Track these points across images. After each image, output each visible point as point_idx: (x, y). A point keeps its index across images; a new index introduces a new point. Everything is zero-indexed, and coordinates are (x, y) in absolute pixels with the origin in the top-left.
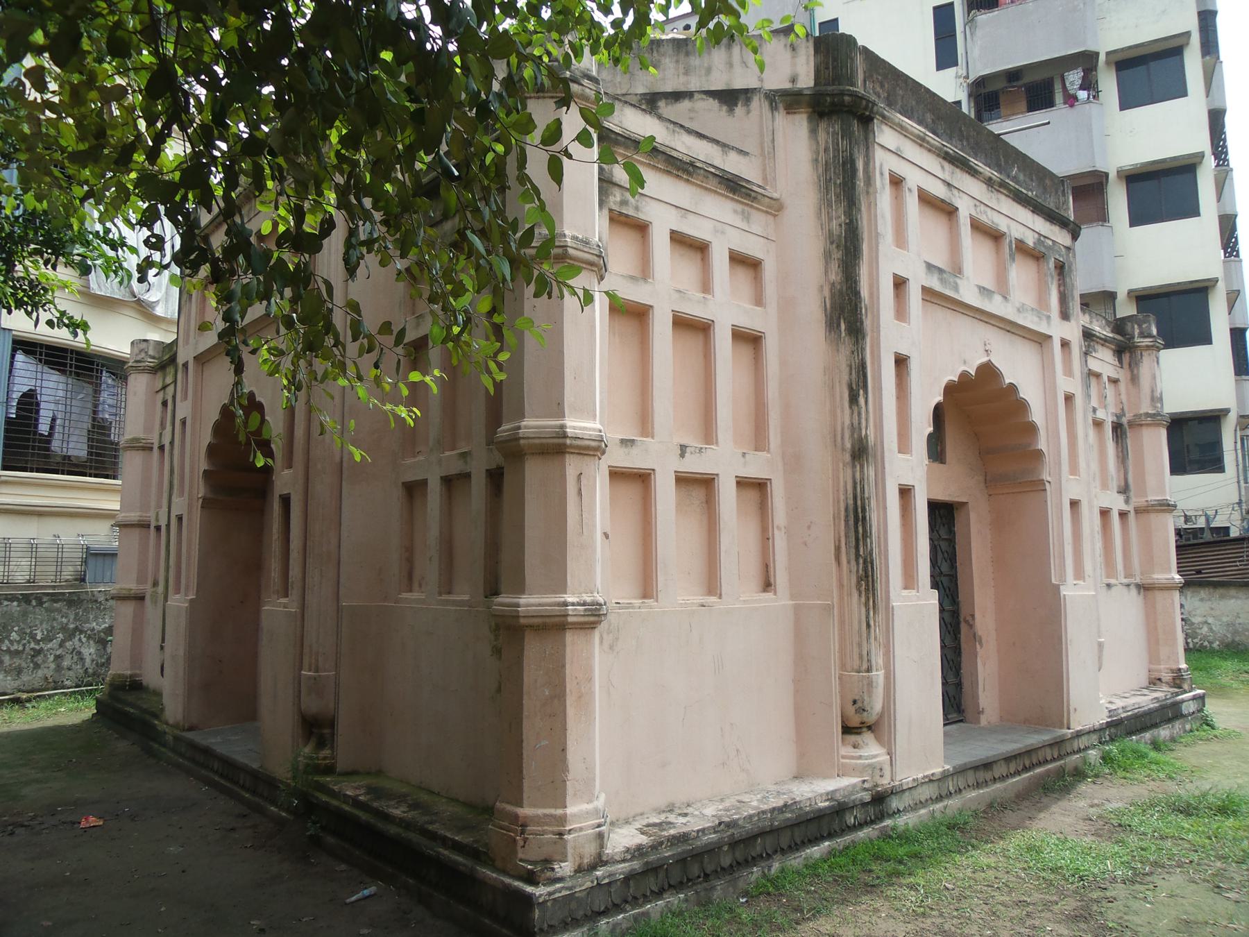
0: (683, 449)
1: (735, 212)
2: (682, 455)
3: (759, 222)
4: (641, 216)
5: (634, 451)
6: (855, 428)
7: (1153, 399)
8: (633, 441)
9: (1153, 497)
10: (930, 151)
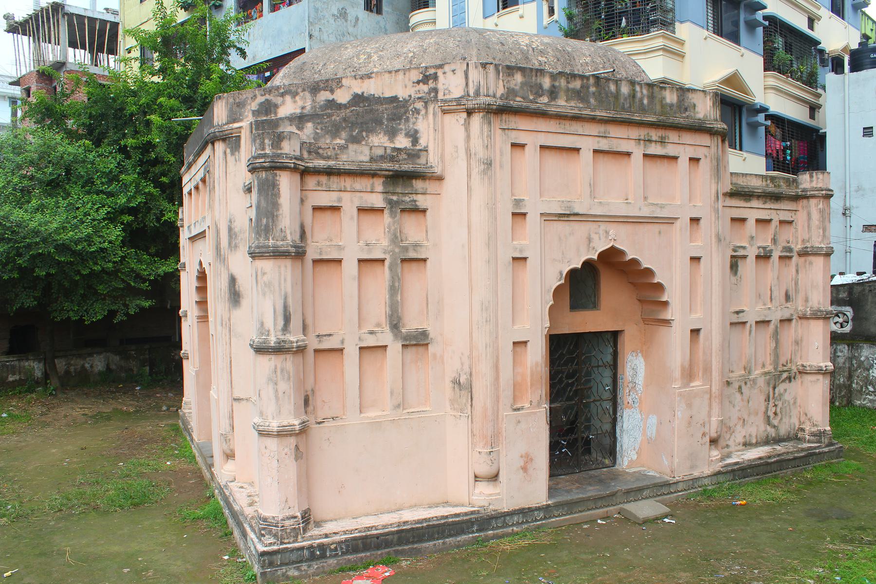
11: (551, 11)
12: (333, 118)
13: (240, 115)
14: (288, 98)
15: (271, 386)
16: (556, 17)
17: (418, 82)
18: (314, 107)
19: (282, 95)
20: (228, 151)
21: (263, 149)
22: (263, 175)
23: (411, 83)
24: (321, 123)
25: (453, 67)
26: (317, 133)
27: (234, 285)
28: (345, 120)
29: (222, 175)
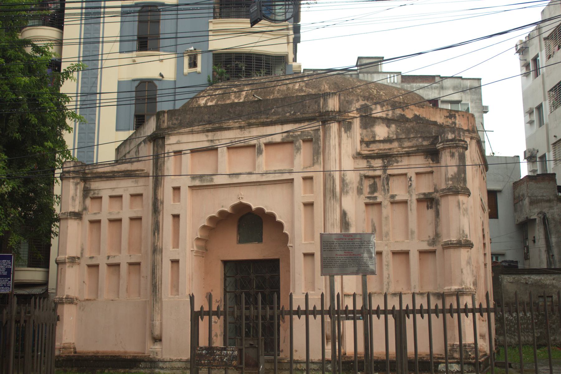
0: (109, 257)
1: (133, 182)
2: (108, 259)
3: (142, 181)
4: (99, 195)
5: (93, 260)
6: (154, 243)
7: (447, 180)
8: (93, 257)
11: (193, 64)
13: (349, 109)
14: (379, 107)
15: (468, 267)
16: (199, 69)
17: (447, 117)
18: (392, 116)
19: (376, 104)
20: (343, 129)
21: (460, 137)
22: (461, 150)
23: (443, 117)
24: (400, 126)
25: (463, 114)
26: (397, 132)
27: (345, 217)
28: (413, 128)
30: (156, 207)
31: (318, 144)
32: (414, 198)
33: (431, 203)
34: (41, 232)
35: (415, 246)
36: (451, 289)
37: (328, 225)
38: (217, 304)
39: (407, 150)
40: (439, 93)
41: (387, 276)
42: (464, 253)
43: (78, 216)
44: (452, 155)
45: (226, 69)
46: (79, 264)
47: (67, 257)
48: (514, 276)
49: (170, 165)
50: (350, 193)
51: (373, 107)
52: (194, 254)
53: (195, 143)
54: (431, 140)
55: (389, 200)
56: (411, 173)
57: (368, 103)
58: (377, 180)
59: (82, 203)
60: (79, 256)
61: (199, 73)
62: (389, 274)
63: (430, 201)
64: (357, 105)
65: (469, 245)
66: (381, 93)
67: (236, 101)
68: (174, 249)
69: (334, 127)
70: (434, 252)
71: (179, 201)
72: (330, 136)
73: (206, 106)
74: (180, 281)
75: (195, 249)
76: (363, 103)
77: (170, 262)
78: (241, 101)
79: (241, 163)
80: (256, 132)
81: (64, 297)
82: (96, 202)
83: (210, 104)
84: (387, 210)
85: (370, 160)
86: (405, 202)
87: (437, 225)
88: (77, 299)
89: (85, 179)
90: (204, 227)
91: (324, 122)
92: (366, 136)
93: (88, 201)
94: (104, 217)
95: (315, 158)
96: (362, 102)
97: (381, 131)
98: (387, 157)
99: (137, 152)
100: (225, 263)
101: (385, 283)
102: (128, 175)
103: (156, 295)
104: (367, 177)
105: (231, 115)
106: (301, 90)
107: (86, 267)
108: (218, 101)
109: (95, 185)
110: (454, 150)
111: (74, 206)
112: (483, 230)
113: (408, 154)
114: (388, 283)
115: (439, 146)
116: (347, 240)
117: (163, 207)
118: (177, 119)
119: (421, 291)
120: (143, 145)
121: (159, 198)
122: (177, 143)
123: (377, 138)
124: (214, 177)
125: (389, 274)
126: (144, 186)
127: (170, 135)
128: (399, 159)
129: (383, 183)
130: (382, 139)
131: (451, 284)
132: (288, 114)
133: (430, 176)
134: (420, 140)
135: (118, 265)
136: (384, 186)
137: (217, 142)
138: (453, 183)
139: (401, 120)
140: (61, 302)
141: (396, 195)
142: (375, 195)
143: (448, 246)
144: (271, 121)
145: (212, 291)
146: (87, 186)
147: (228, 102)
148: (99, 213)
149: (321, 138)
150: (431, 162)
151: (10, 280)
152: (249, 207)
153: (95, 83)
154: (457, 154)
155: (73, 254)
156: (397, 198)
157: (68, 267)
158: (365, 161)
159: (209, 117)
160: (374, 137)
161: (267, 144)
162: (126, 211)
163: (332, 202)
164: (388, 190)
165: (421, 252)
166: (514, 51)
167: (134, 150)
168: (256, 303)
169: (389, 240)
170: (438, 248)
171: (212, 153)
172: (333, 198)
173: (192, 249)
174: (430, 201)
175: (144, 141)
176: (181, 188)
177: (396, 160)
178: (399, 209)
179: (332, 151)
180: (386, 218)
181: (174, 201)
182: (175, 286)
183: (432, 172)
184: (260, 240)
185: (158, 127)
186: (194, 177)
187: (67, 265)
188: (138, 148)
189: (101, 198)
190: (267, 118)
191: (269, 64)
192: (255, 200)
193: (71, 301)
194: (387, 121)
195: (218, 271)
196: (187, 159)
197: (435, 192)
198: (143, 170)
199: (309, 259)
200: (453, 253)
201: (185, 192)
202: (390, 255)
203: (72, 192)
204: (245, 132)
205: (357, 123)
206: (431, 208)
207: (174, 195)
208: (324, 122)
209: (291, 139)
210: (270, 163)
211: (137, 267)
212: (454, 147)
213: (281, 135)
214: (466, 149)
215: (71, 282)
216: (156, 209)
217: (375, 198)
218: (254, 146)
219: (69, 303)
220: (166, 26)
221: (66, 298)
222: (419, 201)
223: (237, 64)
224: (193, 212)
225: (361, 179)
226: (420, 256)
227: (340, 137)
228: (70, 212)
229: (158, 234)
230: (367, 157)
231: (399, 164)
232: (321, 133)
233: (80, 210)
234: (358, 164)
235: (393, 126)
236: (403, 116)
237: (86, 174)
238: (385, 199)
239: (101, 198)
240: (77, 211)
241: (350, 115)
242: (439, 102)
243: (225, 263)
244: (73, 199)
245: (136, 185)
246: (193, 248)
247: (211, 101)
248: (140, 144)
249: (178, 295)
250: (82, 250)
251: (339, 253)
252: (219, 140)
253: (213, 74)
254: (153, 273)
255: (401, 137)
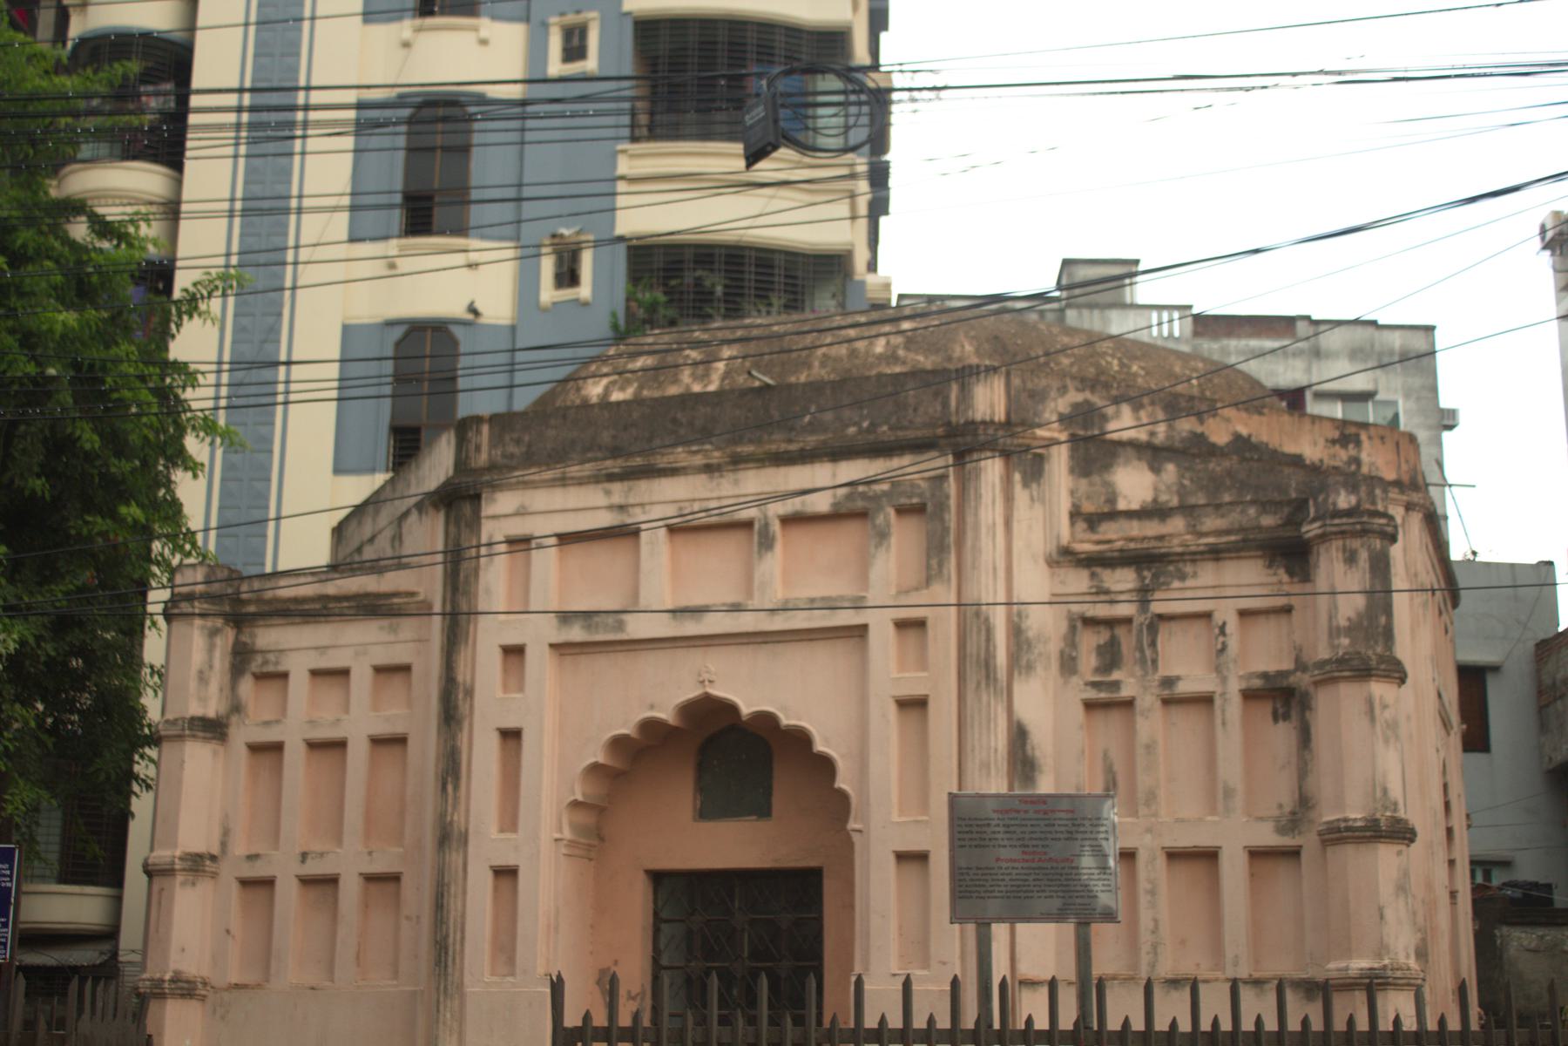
0: (304, 856)
1: (381, 628)
2: (303, 861)
3: (408, 628)
4: (281, 668)
5: (259, 863)
7: (1334, 632)
9: (1329, 817)
10: (580, 484)
11: (568, 276)
12: (1211, 466)
13: (1035, 414)
14: (1126, 410)
16: (585, 291)
17: (1334, 442)
18: (1168, 438)
19: (1117, 401)
20: (1017, 477)
21: (1374, 503)
22: (1377, 544)
23: (1321, 442)
24: (1187, 469)
26: (1182, 486)
29: (1000, 521)
30: (452, 709)
31: (942, 520)
32: (1235, 686)
33: (1287, 704)
34: (102, 777)
35: (1235, 835)
36: (1347, 969)
37: (972, 766)
38: (632, 1007)
39: (1211, 540)
40: (1308, 370)
41: (1151, 925)
42: (1386, 857)
43: (213, 729)
44: (1351, 559)
45: (665, 293)
46: (214, 875)
47: (178, 853)
48: (1540, 932)
49: (494, 580)
50: (1040, 670)
51: (1110, 410)
52: (564, 851)
53: (571, 515)
54: (1286, 510)
55: (1156, 691)
56: (1226, 612)
57: (1097, 400)
58: (1120, 632)
59: (227, 692)
60: (215, 850)
61: (586, 304)
62: (1156, 921)
63: (1281, 697)
64: (1063, 404)
65: (1402, 833)
66: (1135, 368)
67: (697, 388)
68: (502, 836)
69: (992, 470)
70: (1294, 854)
71: (521, 689)
72: (978, 497)
73: (605, 404)
74: (520, 931)
75: (567, 834)
76: (1079, 397)
77: (490, 874)
78: (712, 388)
79: (711, 575)
80: (754, 482)
81: (167, 977)
82: (272, 688)
83: (616, 396)
84: (1151, 723)
85: (1099, 570)
86: (1205, 701)
87: (1303, 771)
88: (205, 984)
89: (238, 620)
90: (595, 768)
91: (961, 456)
92: (1088, 498)
93: (246, 686)
94: (293, 735)
95: (934, 562)
96: (1074, 396)
97: (1134, 484)
98: (1151, 563)
99: (398, 538)
100: (658, 878)
101: (1145, 948)
102: (371, 607)
103: (446, 975)
104: (1090, 622)
105: (682, 432)
106: (891, 357)
107: (235, 886)
108: (641, 387)
109: (268, 637)
110: (1355, 543)
111: (203, 700)
112: (1445, 786)
113: (1216, 554)
114: (1155, 947)
115: (1311, 530)
116: (1031, 815)
117: (472, 706)
118: (518, 442)
119: (1256, 975)
120: (414, 516)
121: (460, 678)
122: (517, 514)
123: (1122, 505)
124: (626, 617)
125: (1156, 921)
126: (414, 643)
127: (495, 487)
128: (1189, 569)
129: (1139, 641)
130: (1135, 506)
131: (1348, 953)
132: (852, 430)
133: (1283, 619)
134: (1252, 511)
135: (332, 881)
136: (1142, 651)
137: (638, 510)
138: (1352, 644)
139: (1194, 450)
140: (158, 992)
141: (1178, 678)
142: (1116, 675)
143: (1339, 835)
144: (802, 450)
145: (616, 962)
146: (245, 638)
147: (673, 390)
148: (278, 722)
149: (953, 502)
150: (1285, 578)
151: (5, 925)
152: (732, 708)
153: (274, 331)
154: (1363, 555)
155: (199, 847)
156: (1183, 688)
157: (183, 884)
158: (1084, 574)
159: (614, 437)
160: (1112, 499)
161: (788, 521)
162: (361, 717)
163: (985, 698)
164: (1154, 662)
165: (1257, 855)
166: (1537, 243)
167: (388, 533)
168: (752, 1002)
169: (1155, 815)
170: (1308, 841)
171: (623, 545)
172: (988, 685)
173: (557, 836)
174: (1281, 697)
175: (419, 506)
176: (529, 652)
177: (1179, 570)
178: (1187, 722)
179: (985, 541)
180: (1148, 747)
181: (506, 688)
182: (506, 948)
183: (1287, 610)
184: (763, 810)
185: (461, 465)
186: (565, 617)
187: (179, 878)
188: (400, 526)
189: (284, 676)
190: (790, 441)
191: (795, 278)
192: (751, 687)
193: (186, 989)
194: (1153, 454)
195: (637, 901)
196: (546, 562)
197: (1296, 670)
198: (412, 594)
199: (912, 869)
200: (1350, 856)
201: (538, 660)
202: (1161, 861)
203: (198, 657)
204: (723, 481)
205: (1059, 461)
206: (1286, 717)
207: (505, 670)
208: (961, 456)
209: (860, 504)
210: (797, 576)
211: (390, 887)
212: (1355, 534)
213: (830, 492)
214: (1393, 539)
215: (190, 931)
216: (451, 713)
217: (1115, 685)
218: (748, 525)
219: (182, 996)
220: (490, 164)
221: (172, 981)
222: (1249, 695)
223: (699, 278)
224: (559, 722)
225: (1072, 629)
226: (1251, 865)
227: (1009, 499)
228: (193, 719)
229: (456, 787)
230: (1092, 562)
231: (1189, 583)
232: (952, 487)
233: (223, 709)
234: (1063, 583)
235: (1171, 468)
236: (1199, 439)
237: (243, 604)
238: (1145, 689)
239: (284, 676)
240: (211, 714)
241: (1040, 432)
242: (1308, 396)
243: (658, 878)
244: (202, 678)
245: (392, 638)
246: (560, 830)
247: (622, 389)
248: (406, 514)
249: (513, 974)
250: (226, 833)
251: (1004, 853)
252: (642, 505)
253: (628, 308)
254: (439, 905)
255: (1192, 500)
